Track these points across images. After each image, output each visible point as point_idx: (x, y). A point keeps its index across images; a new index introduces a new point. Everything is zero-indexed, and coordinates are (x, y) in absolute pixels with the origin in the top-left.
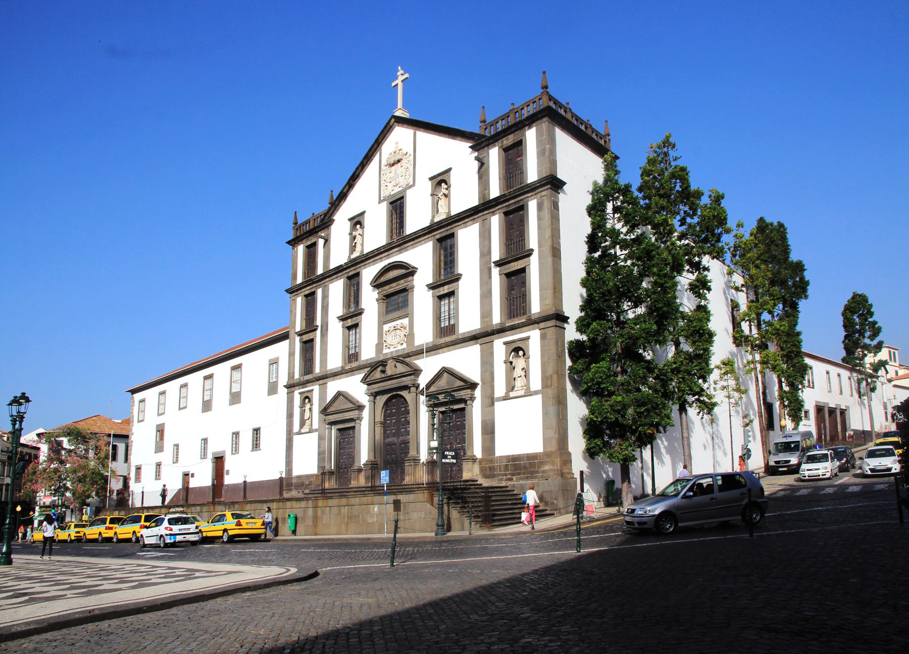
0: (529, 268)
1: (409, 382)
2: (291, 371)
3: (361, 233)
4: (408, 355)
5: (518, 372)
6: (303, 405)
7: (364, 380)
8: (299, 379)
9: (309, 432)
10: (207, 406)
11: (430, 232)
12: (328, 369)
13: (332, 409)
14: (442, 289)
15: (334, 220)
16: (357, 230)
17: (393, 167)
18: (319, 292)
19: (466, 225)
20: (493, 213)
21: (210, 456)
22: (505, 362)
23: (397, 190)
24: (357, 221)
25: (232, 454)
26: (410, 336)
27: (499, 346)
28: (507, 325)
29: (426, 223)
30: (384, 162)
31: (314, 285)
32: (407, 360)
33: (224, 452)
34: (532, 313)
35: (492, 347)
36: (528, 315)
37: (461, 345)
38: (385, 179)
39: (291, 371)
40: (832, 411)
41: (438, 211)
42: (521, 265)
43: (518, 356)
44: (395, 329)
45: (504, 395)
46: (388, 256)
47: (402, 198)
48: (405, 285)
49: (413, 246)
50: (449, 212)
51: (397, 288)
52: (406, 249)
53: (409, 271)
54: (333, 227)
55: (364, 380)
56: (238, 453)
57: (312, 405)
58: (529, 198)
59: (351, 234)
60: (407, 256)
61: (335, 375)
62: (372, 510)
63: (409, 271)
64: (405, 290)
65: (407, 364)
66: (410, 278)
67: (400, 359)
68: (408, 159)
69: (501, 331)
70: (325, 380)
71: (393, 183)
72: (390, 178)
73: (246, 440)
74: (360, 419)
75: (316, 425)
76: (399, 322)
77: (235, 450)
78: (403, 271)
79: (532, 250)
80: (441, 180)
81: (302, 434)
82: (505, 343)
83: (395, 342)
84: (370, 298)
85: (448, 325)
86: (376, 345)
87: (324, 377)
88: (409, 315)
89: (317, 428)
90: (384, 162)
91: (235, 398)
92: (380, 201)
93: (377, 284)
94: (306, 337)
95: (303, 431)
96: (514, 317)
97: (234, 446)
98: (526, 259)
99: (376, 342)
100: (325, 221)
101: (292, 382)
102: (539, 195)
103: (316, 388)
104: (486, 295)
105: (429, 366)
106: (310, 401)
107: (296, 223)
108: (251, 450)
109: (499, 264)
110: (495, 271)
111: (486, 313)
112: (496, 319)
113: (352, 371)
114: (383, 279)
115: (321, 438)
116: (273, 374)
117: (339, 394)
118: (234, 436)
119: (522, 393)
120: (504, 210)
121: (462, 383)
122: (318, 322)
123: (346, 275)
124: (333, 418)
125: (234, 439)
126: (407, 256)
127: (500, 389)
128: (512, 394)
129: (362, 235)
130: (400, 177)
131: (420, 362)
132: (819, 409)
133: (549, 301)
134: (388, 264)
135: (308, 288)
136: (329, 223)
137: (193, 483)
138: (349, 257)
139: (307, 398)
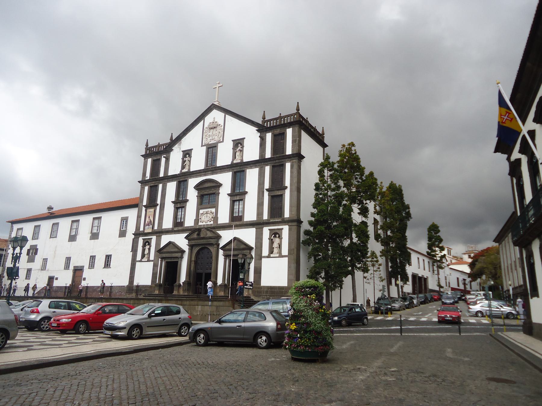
1: (213, 242)
2: (138, 226)
3: (189, 160)
4: (214, 228)
5: (275, 245)
6: (144, 246)
7: (186, 238)
9: (147, 261)
10: (72, 238)
12: (163, 228)
14: (235, 197)
15: (173, 150)
16: (187, 157)
17: (212, 130)
18: (160, 186)
19: (251, 168)
20: (267, 165)
21: (71, 268)
23: (212, 142)
24: (187, 154)
25: (89, 268)
26: (216, 218)
28: (271, 221)
29: (229, 163)
30: (206, 125)
31: (157, 182)
32: (214, 230)
33: (83, 266)
34: (285, 217)
36: (283, 218)
37: (245, 227)
40: (420, 278)
41: (235, 158)
42: (280, 193)
43: (275, 237)
44: (207, 213)
46: (205, 175)
47: (216, 146)
48: (214, 191)
49: (221, 173)
50: (242, 160)
53: (218, 185)
54: (171, 153)
55: (186, 238)
56: (94, 268)
57: (150, 247)
58: (287, 162)
59: (183, 159)
60: (216, 177)
63: (218, 185)
64: (214, 194)
65: (214, 232)
66: (218, 189)
68: (221, 128)
70: (161, 234)
71: (211, 138)
72: (209, 135)
73: (100, 262)
74: (182, 257)
75: (152, 257)
76: (209, 210)
77: (92, 265)
79: (287, 187)
80: (238, 143)
81: (143, 262)
82: (269, 230)
83: (206, 219)
84: (192, 195)
85: (237, 215)
87: (160, 233)
88: (216, 206)
89: (153, 259)
90: (206, 125)
91: (95, 236)
92: (202, 146)
93: (197, 187)
95: (143, 260)
96: (275, 218)
97: (91, 264)
100: (167, 149)
102: (292, 161)
103: (154, 238)
104: (260, 204)
105: (226, 236)
106: (149, 244)
108: (103, 267)
109: (267, 190)
110: (266, 194)
112: (265, 217)
113: (178, 232)
114: (201, 187)
116: (123, 226)
117: (170, 243)
118: (91, 258)
119: (278, 255)
120: (273, 165)
122: (159, 202)
123: (178, 180)
124: (164, 255)
125: (91, 260)
126: (216, 177)
127: (265, 251)
128: (272, 255)
129: (190, 161)
131: (221, 233)
132: (414, 276)
133: (294, 213)
134: (205, 179)
135: (153, 182)
136: (170, 151)
137: (56, 284)
138: (181, 171)
139: (147, 243)
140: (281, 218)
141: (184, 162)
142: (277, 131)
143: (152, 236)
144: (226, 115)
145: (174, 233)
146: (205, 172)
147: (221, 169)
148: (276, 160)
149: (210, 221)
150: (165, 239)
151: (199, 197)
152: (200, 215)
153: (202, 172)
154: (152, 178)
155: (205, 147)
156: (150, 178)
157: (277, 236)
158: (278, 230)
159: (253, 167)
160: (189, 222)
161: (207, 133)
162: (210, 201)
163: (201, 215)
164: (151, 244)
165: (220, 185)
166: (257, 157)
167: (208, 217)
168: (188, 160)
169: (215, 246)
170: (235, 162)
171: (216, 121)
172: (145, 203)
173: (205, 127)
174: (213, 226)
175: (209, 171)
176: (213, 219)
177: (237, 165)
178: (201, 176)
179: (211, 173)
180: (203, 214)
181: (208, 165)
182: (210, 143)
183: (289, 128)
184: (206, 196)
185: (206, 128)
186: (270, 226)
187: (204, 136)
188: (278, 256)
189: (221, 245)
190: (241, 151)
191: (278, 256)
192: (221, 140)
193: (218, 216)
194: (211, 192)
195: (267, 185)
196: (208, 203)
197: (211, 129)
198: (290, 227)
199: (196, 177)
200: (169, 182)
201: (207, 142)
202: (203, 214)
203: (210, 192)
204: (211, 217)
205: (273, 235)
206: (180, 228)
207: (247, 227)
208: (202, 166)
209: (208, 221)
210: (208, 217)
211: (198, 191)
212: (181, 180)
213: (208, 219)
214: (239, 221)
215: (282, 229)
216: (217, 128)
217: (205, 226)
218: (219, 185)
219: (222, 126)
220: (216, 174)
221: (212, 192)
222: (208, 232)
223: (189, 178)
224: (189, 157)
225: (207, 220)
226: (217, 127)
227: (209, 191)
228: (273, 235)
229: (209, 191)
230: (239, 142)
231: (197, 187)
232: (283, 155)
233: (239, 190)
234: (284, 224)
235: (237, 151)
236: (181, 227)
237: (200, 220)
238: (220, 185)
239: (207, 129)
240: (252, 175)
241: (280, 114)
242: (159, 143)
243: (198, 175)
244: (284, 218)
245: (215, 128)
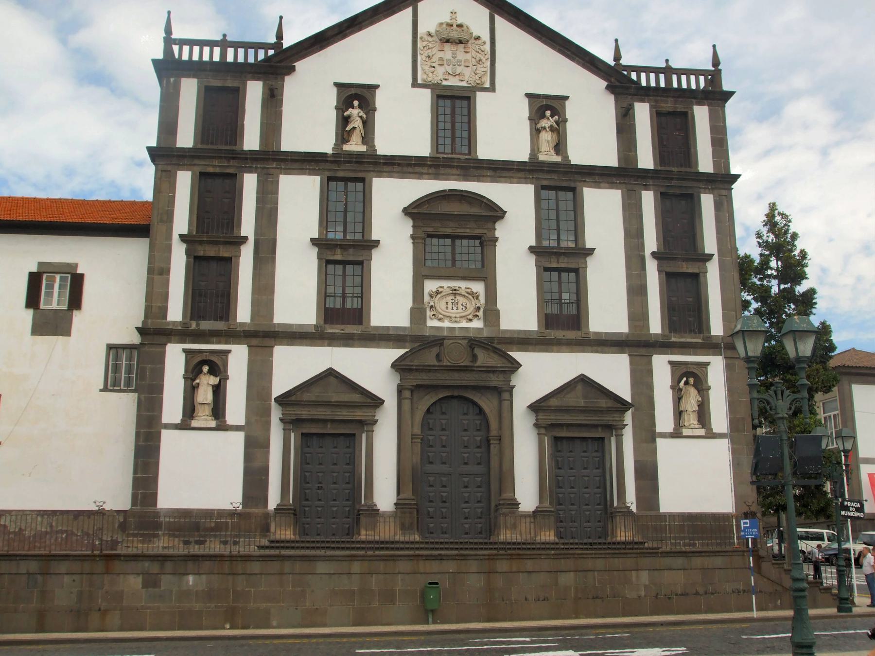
0: (706, 277)
4: (491, 340)
8: (183, 323)
11: (531, 171)
13: (307, 397)
14: (554, 259)
17: (447, 46)
19: (597, 185)
20: (646, 188)
22: (672, 387)
23: (453, 82)
26: (491, 313)
28: (673, 339)
31: (232, 163)
35: (650, 363)
36: (706, 334)
38: (430, 55)
39: (157, 304)
44: (455, 292)
45: (672, 431)
46: (437, 177)
47: (468, 98)
49: (494, 179)
51: (459, 230)
52: (479, 178)
54: (287, 79)
57: (224, 378)
62: (634, 579)
63: (495, 213)
66: (490, 225)
67: (474, 343)
69: (662, 345)
70: (268, 342)
71: (449, 69)
72: (441, 59)
74: (368, 424)
76: (462, 285)
78: (475, 210)
83: (453, 313)
86: (412, 309)
92: (415, 84)
94: (201, 251)
98: (701, 264)
99: (409, 303)
101: (157, 323)
102: (716, 191)
107: (168, 30)
112: (656, 326)
113: (348, 340)
114: (425, 209)
120: (663, 190)
121: (610, 403)
127: (664, 420)
130: (462, 67)
131: (517, 355)
134: (450, 190)
140: (701, 335)
141: (343, 121)
142: (668, 105)
143: (226, 343)
144: (497, 18)
145: (326, 342)
146: (437, 167)
147: (495, 169)
148: (672, 179)
149: (471, 320)
151: (420, 241)
152: (426, 298)
153: (424, 165)
154: (205, 147)
155: (428, 92)
156: (199, 146)
157: (691, 380)
158: (695, 366)
159: (602, 185)
161: (435, 50)
162: (458, 257)
163: (431, 296)
164: (226, 371)
167: (460, 307)
168: (361, 117)
169: (506, 395)
170: (542, 157)
171: (459, 22)
172: (181, 223)
173: (422, 30)
174: (485, 336)
175: (452, 167)
176: (481, 313)
177: (552, 168)
178: (420, 176)
179: (458, 175)
180: (441, 292)
181: (441, 149)
182: (445, 83)
183: (700, 104)
184: (442, 241)
185: (429, 34)
186: (672, 354)
187: (419, 58)
188: (704, 434)
190: (559, 131)
191: (704, 434)
192: (487, 85)
193: (500, 305)
194: (467, 231)
195: (651, 242)
196: (449, 263)
197: (448, 41)
198: (730, 361)
199: (403, 175)
200: (288, 171)
201: (439, 76)
202: (438, 293)
203: (463, 230)
204: (471, 309)
205: (685, 379)
206: (351, 329)
207: (599, 349)
208: (422, 147)
209: (461, 317)
210: (460, 307)
211: (413, 219)
212: (341, 174)
213: (460, 310)
214: (573, 329)
215: (708, 364)
216: (469, 45)
217: (457, 333)
218: (495, 213)
219: (485, 43)
220: (479, 181)
221: (468, 231)
222: (479, 352)
223: (375, 174)
224: (360, 107)
225: (458, 315)
226: (468, 41)
227: (421, 225)
228: (685, 379)
229: (439, 225)
230: (549, 103)
232: (693, 170)
233: (559, 239)
234: (711, 351)
235: (544, 128)
236: (355, 327)
237: (429, 313)
239: (430, 39)
241: (667, 61)
242: (225, 36)
243: (410, 169)
244: (710, 337)
245: (460, 42)
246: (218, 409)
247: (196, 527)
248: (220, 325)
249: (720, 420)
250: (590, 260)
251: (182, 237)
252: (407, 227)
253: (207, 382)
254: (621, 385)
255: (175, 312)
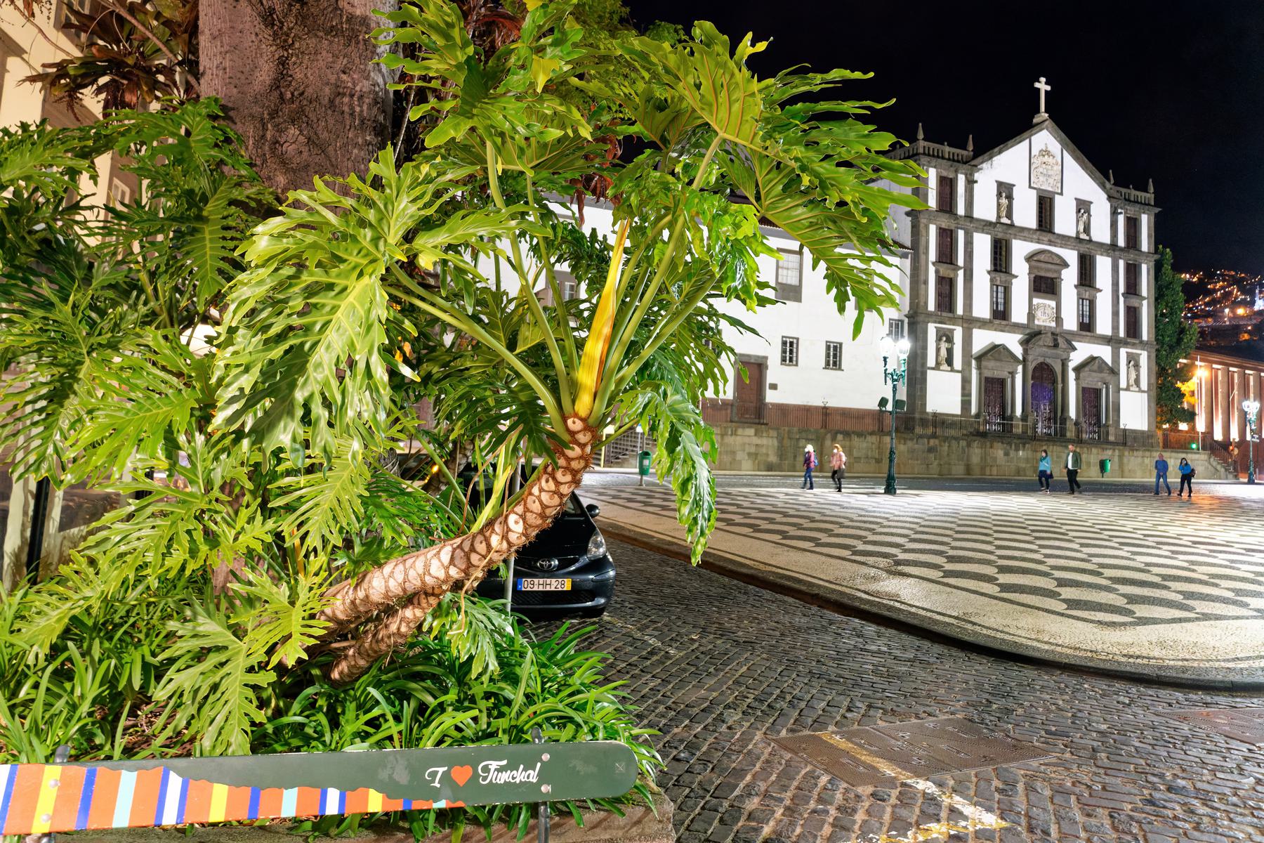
6: (939, 339)
18: (961, 234)
24: (1005, 190)
26: (1059, 319)
27: (1123, 352)
46: (1039, 241)
61: (983, 324)
87: (970, 322)
92: (1030, 187)
93: (1029, 259)
104: (1115, 314)
105: (1082, 351)
110: (1122, 299)
111: (1115, 327)
112: (1122, 334)
115: (966, 382)
127: (1123, 384)
150: (983, 339)
160: (1019, 314)
165: (1065, 265)
166: (1107, 239)
189: (1072, 365)
193: (1063, 316)
195: (1122, 289)
224: (1007, 197)
231: (1029, 259)
238: (1065, 265)
240: (1103, 265)
246: (949, 361)
247: (943, 423)
248: (950, 315)
249: (1144, 386)
250: (1098, 295)
251: (934, 264)
252: (1026, 266)
253: (944, 346)
254: (1109, 361)
255: (931, 306)
